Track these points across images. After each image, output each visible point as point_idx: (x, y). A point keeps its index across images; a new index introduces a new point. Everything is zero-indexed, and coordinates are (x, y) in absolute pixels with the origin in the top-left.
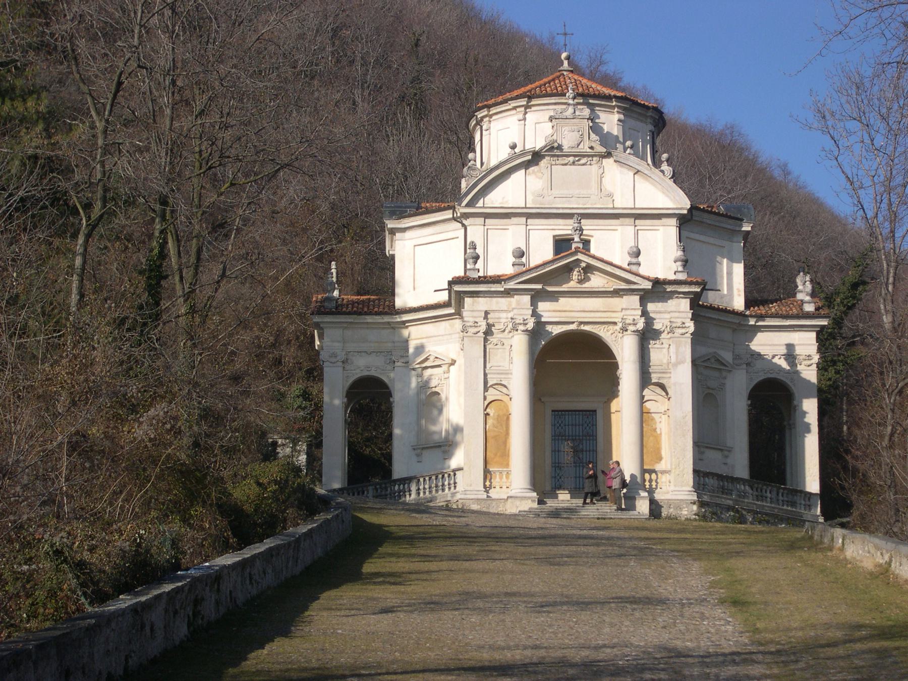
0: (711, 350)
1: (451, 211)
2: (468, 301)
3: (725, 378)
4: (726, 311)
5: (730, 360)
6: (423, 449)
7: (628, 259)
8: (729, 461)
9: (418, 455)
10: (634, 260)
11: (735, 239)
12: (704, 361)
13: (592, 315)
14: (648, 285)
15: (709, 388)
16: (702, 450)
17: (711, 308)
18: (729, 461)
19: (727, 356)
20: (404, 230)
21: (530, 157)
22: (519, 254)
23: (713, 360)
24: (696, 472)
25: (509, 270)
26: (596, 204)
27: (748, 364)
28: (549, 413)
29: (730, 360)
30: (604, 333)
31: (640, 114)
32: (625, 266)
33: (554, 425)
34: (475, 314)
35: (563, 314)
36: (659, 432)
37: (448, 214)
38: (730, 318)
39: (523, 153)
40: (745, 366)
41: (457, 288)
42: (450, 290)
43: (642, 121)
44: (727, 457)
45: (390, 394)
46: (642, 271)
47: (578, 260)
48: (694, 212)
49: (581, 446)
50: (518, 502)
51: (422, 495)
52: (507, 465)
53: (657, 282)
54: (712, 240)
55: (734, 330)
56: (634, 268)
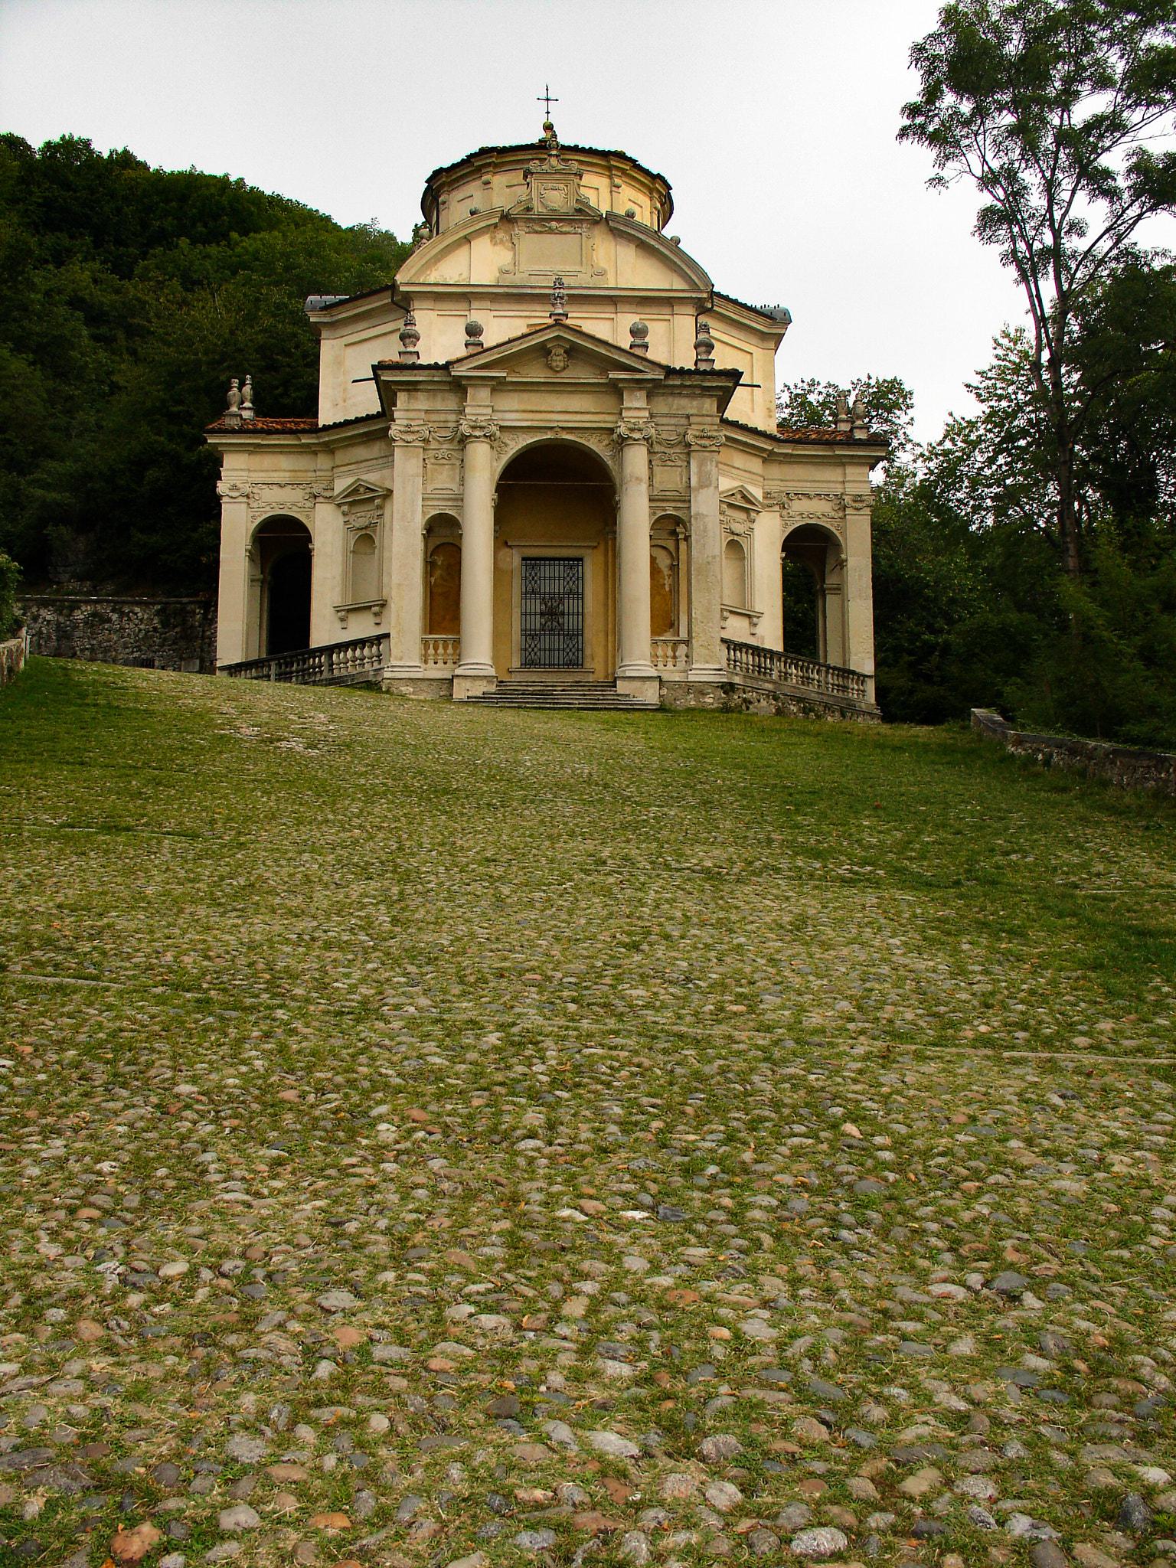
0: (736, 484)
1: (389, 293)
2: (402, 399)
4: (754, 431)
5: (761, 499)
6: (348, 611)
8: (757, 630)
9: (342, 620)
10: (638, 341)
13: (579, 417)
14: (660, 375)
15: (733, 533)
16: (726, 614)
17: (735, 425)
18: (757, 630)
19: (757, 493)
20: (333, 325)
22: (473, 331)
23: (739, 496)
25: (463, 352)
29: (761, 499)
32: (627, 347)
34: (412, 415)
37: (385, 300)
39: (488, 216)
40: (777, 508)
42: (376, 378)
44: (755, 625)
45: (309, 540)
50: (467, 684)
52: (459, 632)
53: (670, 371)
55: (765, 461)
56: (638, 352)
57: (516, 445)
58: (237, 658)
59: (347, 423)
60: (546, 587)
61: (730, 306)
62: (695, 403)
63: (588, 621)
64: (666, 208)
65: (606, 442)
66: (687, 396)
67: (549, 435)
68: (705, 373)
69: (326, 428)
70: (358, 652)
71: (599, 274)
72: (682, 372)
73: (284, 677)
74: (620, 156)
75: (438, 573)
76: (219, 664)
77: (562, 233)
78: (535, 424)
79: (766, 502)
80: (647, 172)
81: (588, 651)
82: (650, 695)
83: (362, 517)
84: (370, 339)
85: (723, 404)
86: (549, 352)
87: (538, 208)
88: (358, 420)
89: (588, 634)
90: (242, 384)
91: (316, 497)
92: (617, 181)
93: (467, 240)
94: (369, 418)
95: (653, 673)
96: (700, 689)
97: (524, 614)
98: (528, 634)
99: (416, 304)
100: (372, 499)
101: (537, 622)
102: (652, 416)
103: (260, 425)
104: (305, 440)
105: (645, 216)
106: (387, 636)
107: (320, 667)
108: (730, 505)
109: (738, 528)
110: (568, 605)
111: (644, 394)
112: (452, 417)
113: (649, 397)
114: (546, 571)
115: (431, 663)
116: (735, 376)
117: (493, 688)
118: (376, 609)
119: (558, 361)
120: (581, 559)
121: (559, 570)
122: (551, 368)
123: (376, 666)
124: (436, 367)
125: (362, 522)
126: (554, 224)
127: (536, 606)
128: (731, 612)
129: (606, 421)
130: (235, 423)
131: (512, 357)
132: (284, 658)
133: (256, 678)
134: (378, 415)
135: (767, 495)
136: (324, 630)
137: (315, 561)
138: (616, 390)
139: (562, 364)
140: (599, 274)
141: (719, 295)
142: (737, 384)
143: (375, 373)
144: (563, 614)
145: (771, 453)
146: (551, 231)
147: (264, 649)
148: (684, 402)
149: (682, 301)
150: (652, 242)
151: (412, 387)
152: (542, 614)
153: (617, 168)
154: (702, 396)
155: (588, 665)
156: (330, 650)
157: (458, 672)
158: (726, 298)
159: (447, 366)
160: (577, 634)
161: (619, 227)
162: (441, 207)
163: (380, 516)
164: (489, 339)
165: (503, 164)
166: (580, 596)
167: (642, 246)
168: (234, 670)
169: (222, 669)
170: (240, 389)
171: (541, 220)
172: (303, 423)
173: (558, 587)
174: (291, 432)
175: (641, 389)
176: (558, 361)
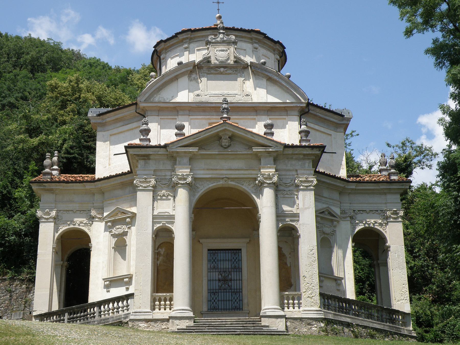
0: (325, 206)
1: (134, 107)
3: (335, 227)
5: (339, 214)
6: (111, 281)
7: (264, 130)
8: (341, 288)
10: (269, 131)
11: (338, 130)
12: (321, 213)
13: (237, 172)
15: (324, 233)
17: (323, 174)
19: (337, 211)
20: (103, 125)
21: (192, 68)
23: (327, 213)
24: (321, 295)
26: (240, 99)
27: (352, 218)
28: (205, 252)
29: (339, 214)
30: (247, 188)
31: (270, 47)
33: (209, 261)
35: (215, 172)
36: (289, 265)
38: (338, 183)
40: (349, 219)
41: (131, 151)
42: (127, 152)
43: (271, 52)
46: (275, 138)
47: (225, 130)
48: (310, 107)
49: (230, 276)
50: (177, 322)
51: (103, 316)
53: (286, 146)
54: (322, 129)
55: (341, 193)
57: (203, 189)
58: (45, 310)
59: (111, 177)
60: (222, 265)
61: (318, 110)
62: (300, 163)
63: (245, 283)
64: (282, 59)
65: (252, 185)
66: (296, 159)
67: (221, 183)
68: (305, 147)
69: (99, 180)
70: (116, 304)
71: (247, 95)
72: (293, 146)
73: (71, 320)
74: (258, 32)
75: (161, 258)
76: (34, 314)
77: (226, 74)
78: (213, 176)
79: (342, 215)
80: (272, 40)
81: (245, 301)
82: (280, 325)
83: (118, 229)
84: (124, 132)
85: (316, 163)
86: (220, 138)
87: (213, 61)
88: (117, 176)
89: (245, 292)
90: (52, 156)
91: (93, 218)
92: (256, 45)
93: (176, 78)
94: (123, 174)
95: (282, 313)
96: (309, 321)
97: (209, 281)
98: (212, 292)
99: (149, 113)
100: (125, 218)
101: (216, 285)
102: (277, 170)
103: (62, 178)
104: (89, 186)
105: (272, 65)
106: (131, 296)
107: (94, 314)
108: (322, 218)
109: (327, 230)
110: (234, 276)
111: (271, 159)
112: (168, 173)
113: (275, 160)
114: (221, 256)
115: (157, 310)
116: (322, 148)
117: (191, 323)
118: (126, 280)
119: (225, 142)
120: (241, 250)
121: (229, 256)
122: (222, 146)
123: (126, 312)
124: (159, 147)
125: (120, 231)
126: (222, 70)
127: (216, 276)
128: (325, 277)
129: (251, 173)
130: (48, 178)
131: (200, 142)
132: (73, 309)
133: (56, 321)
134: (129, 173)
135: (343, 212)
136: (96, 292)
137: (92, 253)
138: (258, 157)
139: (227, 144)
140: (247, 95)
141: (313, 105)
142: (323, 152)
143: (126, 151)
144: (231, 280)
145: (344, 188)
146: (221, 73)
147: (62, 304)
148: (294, 162)
149: (292, 108)
150: (275, 78)
151: (146, 157)
152: (219, 280)
153: (256, 39)
154: (304, 159)
155: (245, 308)
156: (99, 304)
157: (173, 314)
158: (317, 106)
159: (166, 146)
160: (239, 291)
161: (258, 71)
162: (162, 61)
163: (129, 228)
164: (188, 131)
165: (195, 38)
166: (239, 269)
167: (269, 79)
168: (42, 317)
169: (37, 317)
170: (51, 159)
171: (217, 67)
172: (88, 177)
173: (227, 265)
174: (80, 182)
175: (270, 156)
176: (225, 142)
